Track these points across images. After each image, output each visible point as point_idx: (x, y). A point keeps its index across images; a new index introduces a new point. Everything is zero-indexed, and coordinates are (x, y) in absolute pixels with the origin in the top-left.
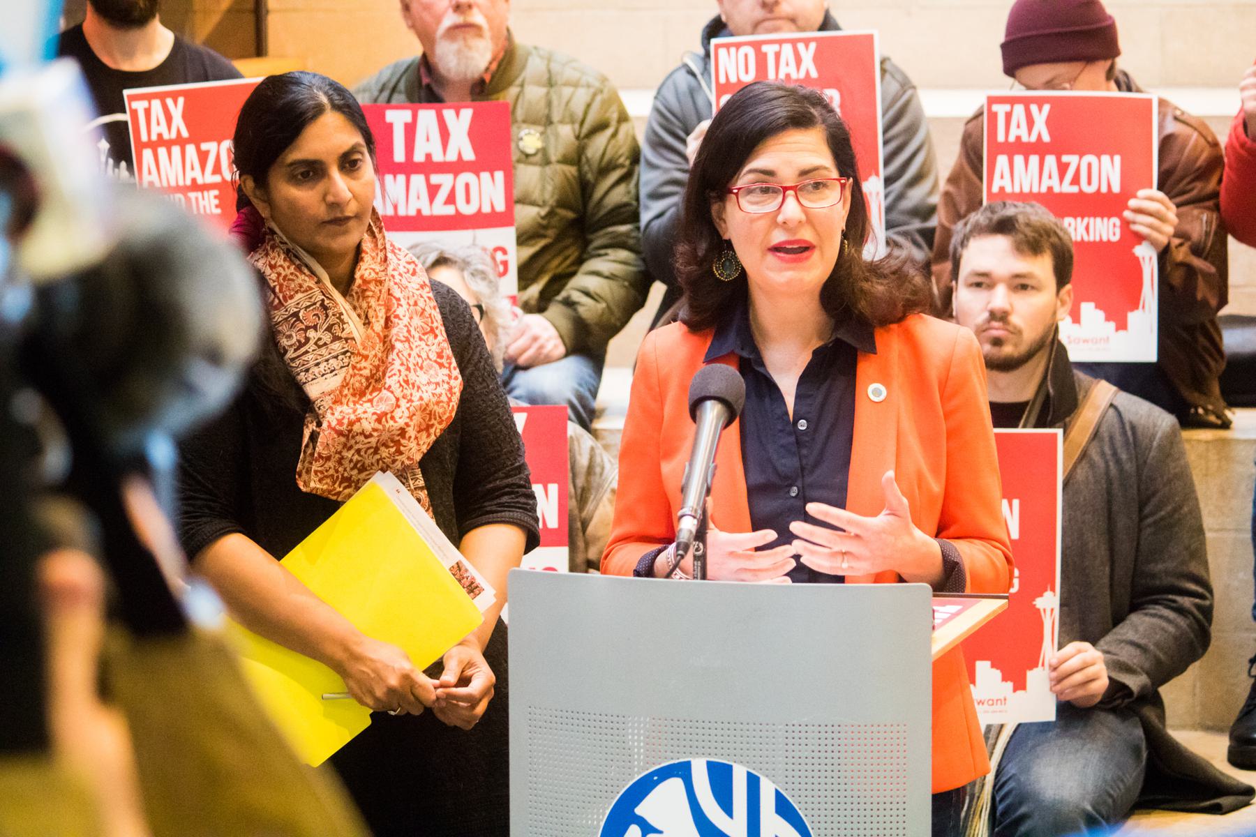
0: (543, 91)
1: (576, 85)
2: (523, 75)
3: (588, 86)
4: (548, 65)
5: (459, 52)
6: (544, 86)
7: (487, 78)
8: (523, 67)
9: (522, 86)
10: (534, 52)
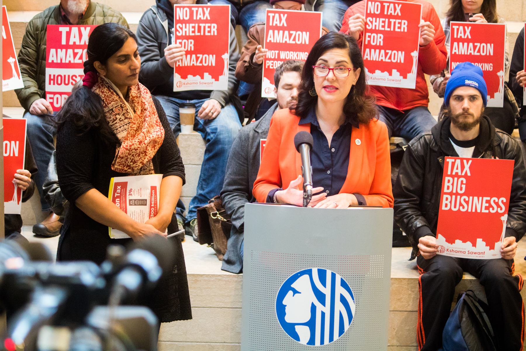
0: (102, 18)
1: (113, 16)
2: (95, 13)
3: (117, 17)
5: (77, 4)
6: (102, 16)
7: (84, 14)
8: (95, 10)
9: (95, 16)
10: (98, 5)
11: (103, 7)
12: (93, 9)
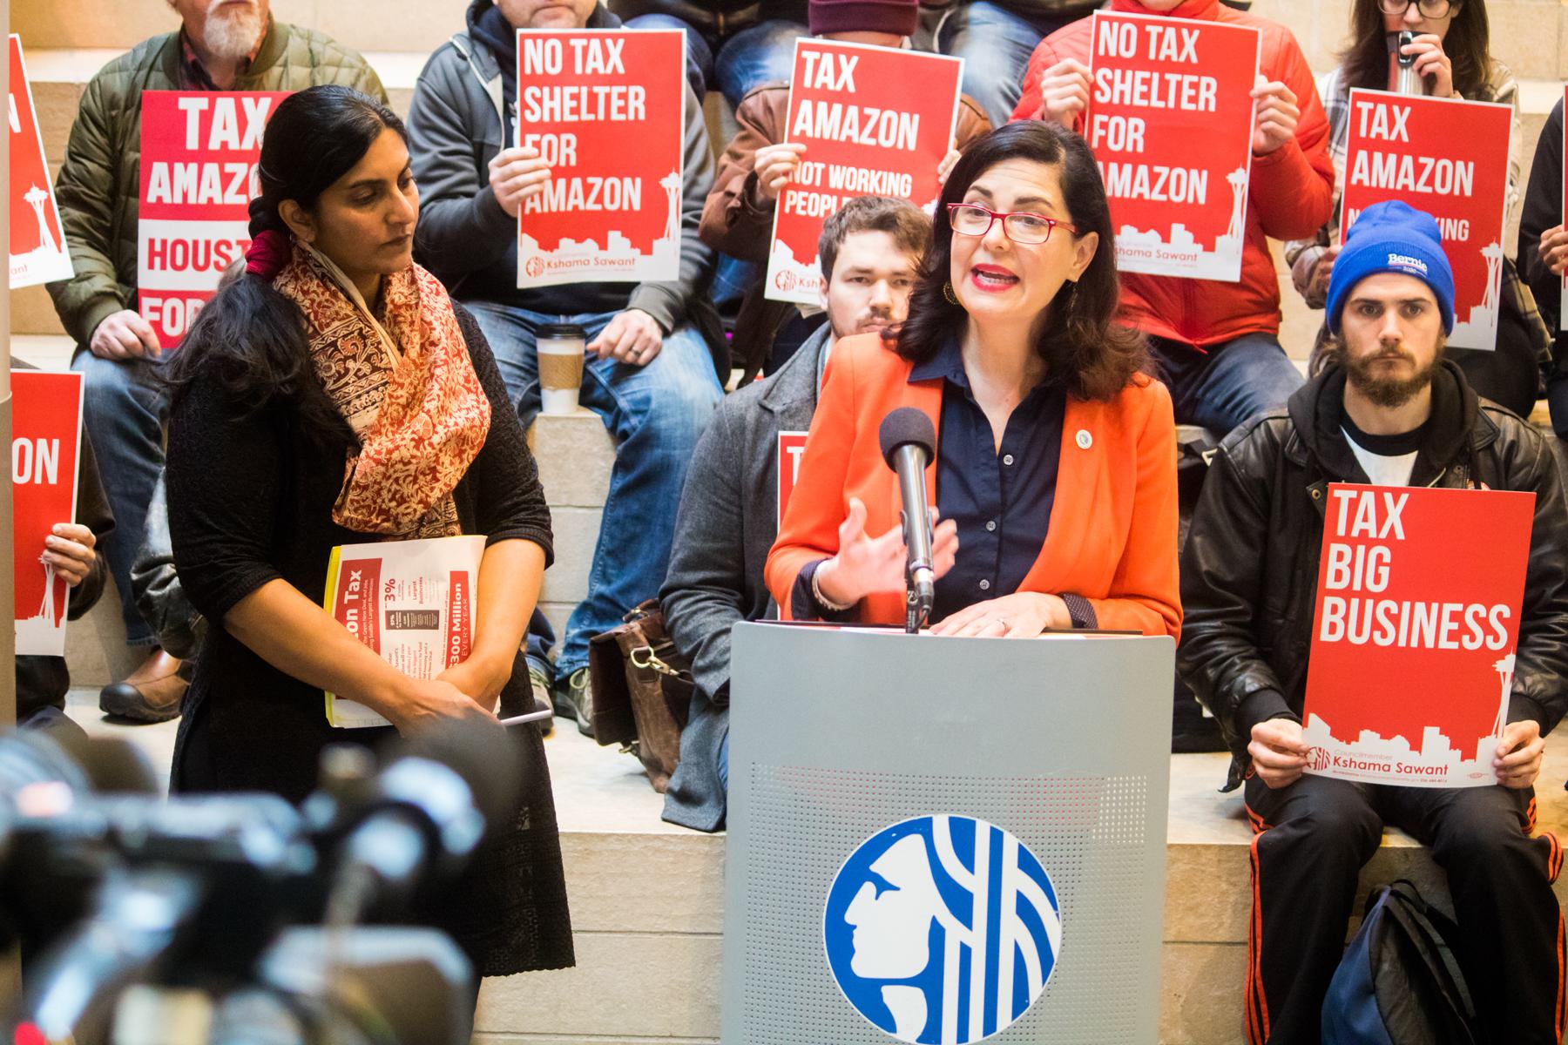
0: (308, 70)
1: (338, 65)
2: (285, 54)
3: (352, 67)
4: (309, 44)
5: (231, 28)
6: (306, 66)
7: (253, 58)
8: (286, 46)
9: (285, 65)
11: (309, 38)
12: (279, 43)
